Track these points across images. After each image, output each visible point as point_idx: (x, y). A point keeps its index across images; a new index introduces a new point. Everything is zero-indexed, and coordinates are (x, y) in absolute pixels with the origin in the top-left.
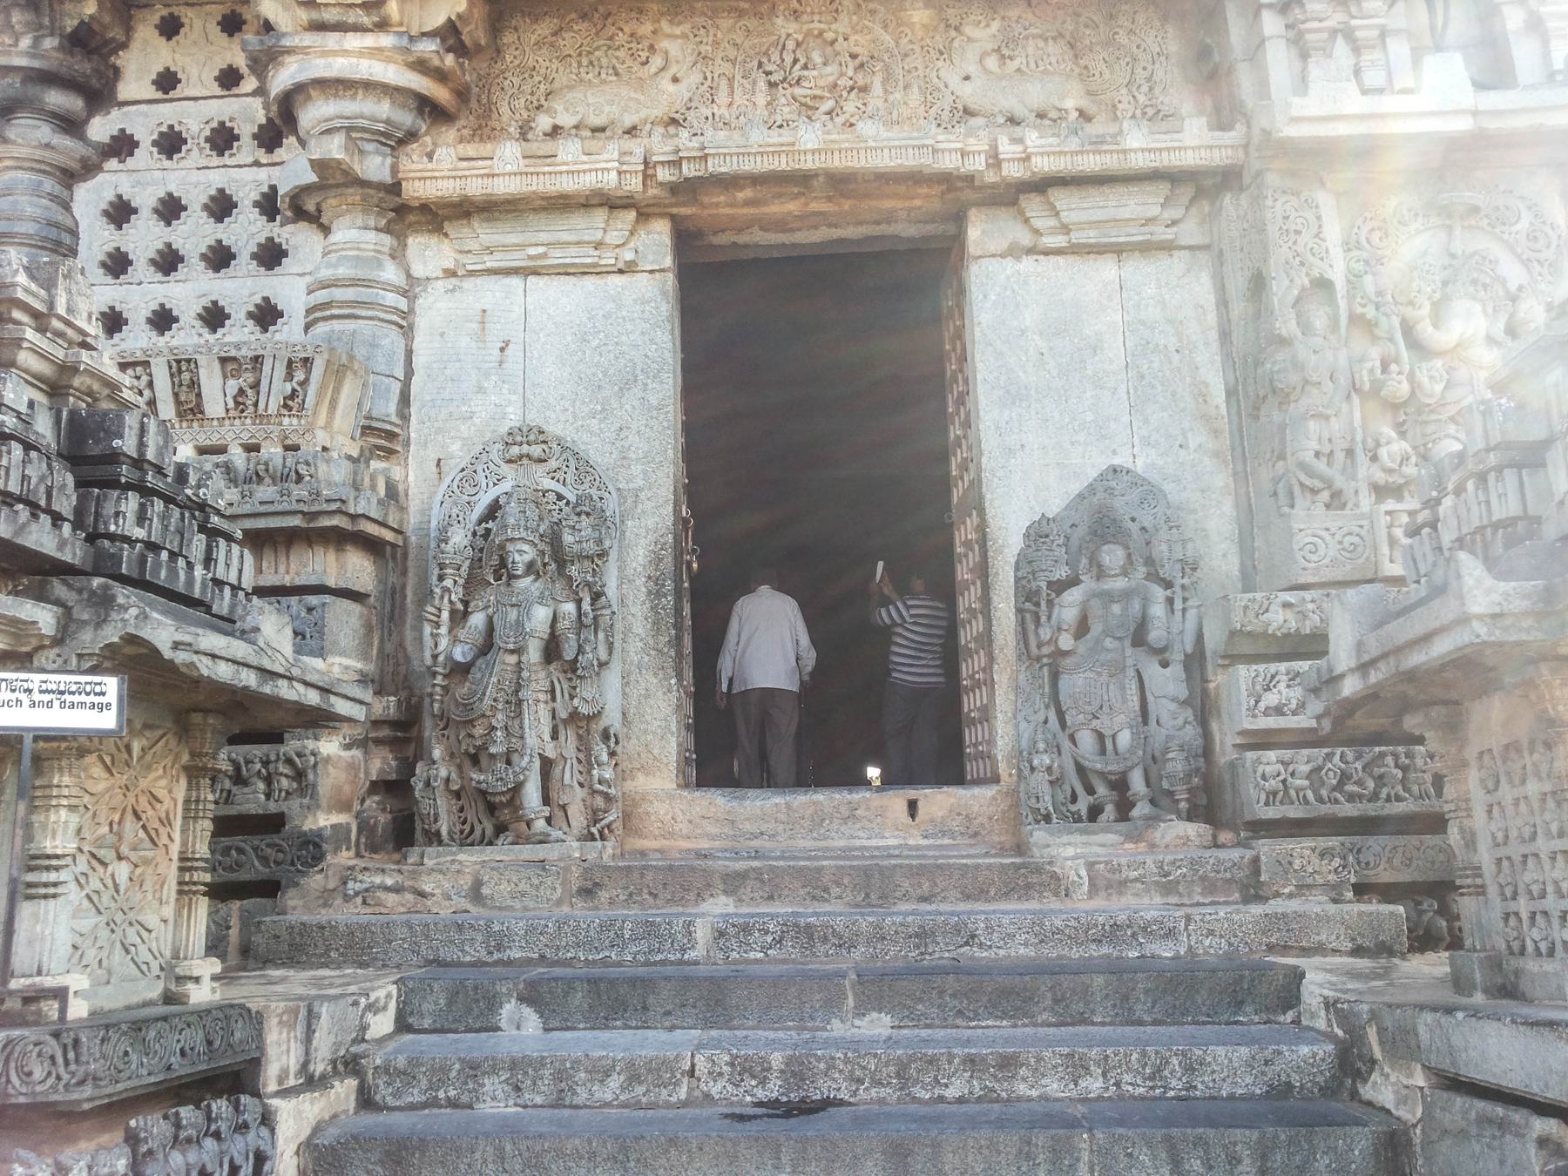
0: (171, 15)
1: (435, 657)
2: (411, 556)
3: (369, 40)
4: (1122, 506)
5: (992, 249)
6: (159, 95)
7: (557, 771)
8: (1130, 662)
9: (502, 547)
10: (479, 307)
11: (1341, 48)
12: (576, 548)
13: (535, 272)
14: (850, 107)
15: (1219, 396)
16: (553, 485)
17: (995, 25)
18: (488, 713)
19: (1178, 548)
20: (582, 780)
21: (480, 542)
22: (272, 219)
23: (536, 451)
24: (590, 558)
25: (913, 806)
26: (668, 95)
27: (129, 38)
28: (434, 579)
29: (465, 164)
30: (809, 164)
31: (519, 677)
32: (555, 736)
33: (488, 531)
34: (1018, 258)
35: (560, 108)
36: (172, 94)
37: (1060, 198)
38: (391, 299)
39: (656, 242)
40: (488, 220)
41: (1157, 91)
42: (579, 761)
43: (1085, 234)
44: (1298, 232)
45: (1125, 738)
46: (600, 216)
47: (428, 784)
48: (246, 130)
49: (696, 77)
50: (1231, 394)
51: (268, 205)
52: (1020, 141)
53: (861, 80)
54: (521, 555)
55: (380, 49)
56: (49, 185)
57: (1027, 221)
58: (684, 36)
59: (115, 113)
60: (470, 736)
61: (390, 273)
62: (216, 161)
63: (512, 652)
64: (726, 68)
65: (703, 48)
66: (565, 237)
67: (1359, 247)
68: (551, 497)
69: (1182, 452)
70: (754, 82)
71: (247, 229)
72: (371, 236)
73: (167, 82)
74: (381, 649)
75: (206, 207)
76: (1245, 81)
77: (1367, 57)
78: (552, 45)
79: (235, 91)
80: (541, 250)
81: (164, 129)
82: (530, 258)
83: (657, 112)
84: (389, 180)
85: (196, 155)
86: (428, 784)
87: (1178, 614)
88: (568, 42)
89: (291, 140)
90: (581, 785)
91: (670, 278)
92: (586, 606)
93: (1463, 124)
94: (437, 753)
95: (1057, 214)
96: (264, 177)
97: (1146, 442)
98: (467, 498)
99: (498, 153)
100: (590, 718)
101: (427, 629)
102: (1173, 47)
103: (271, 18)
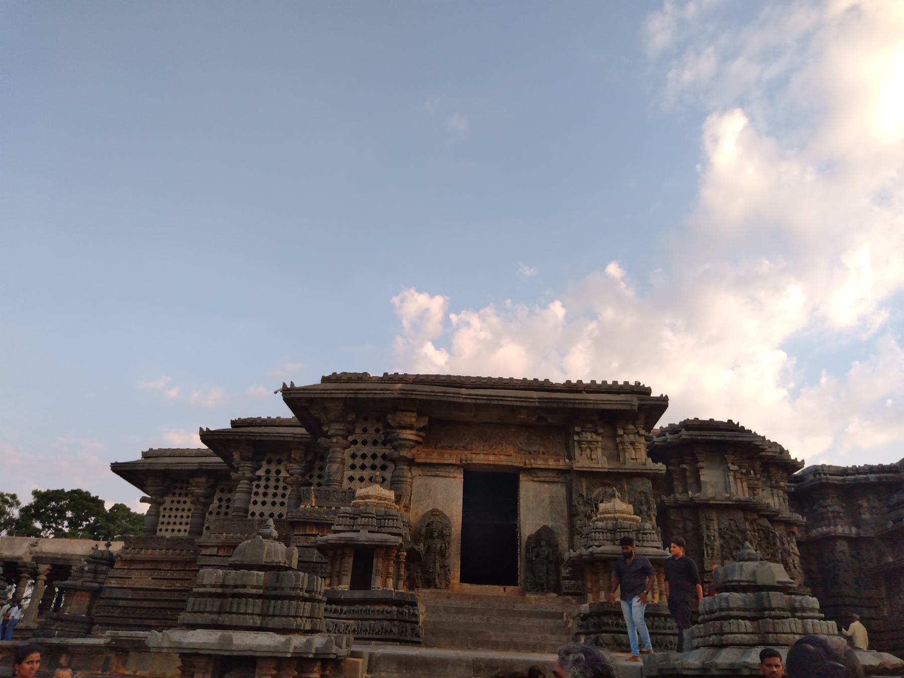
13: (437, 476)
16: (440, 520)
23: (438, 513)
30: (491, 463)
34: (529, 482)
48: (380, 441)
59: (354, 435)
62: (374, 447)
71: (379, 462)
77: (593, 452)
93: (606, 470)
94: (419, 571)
100: (447, 566)
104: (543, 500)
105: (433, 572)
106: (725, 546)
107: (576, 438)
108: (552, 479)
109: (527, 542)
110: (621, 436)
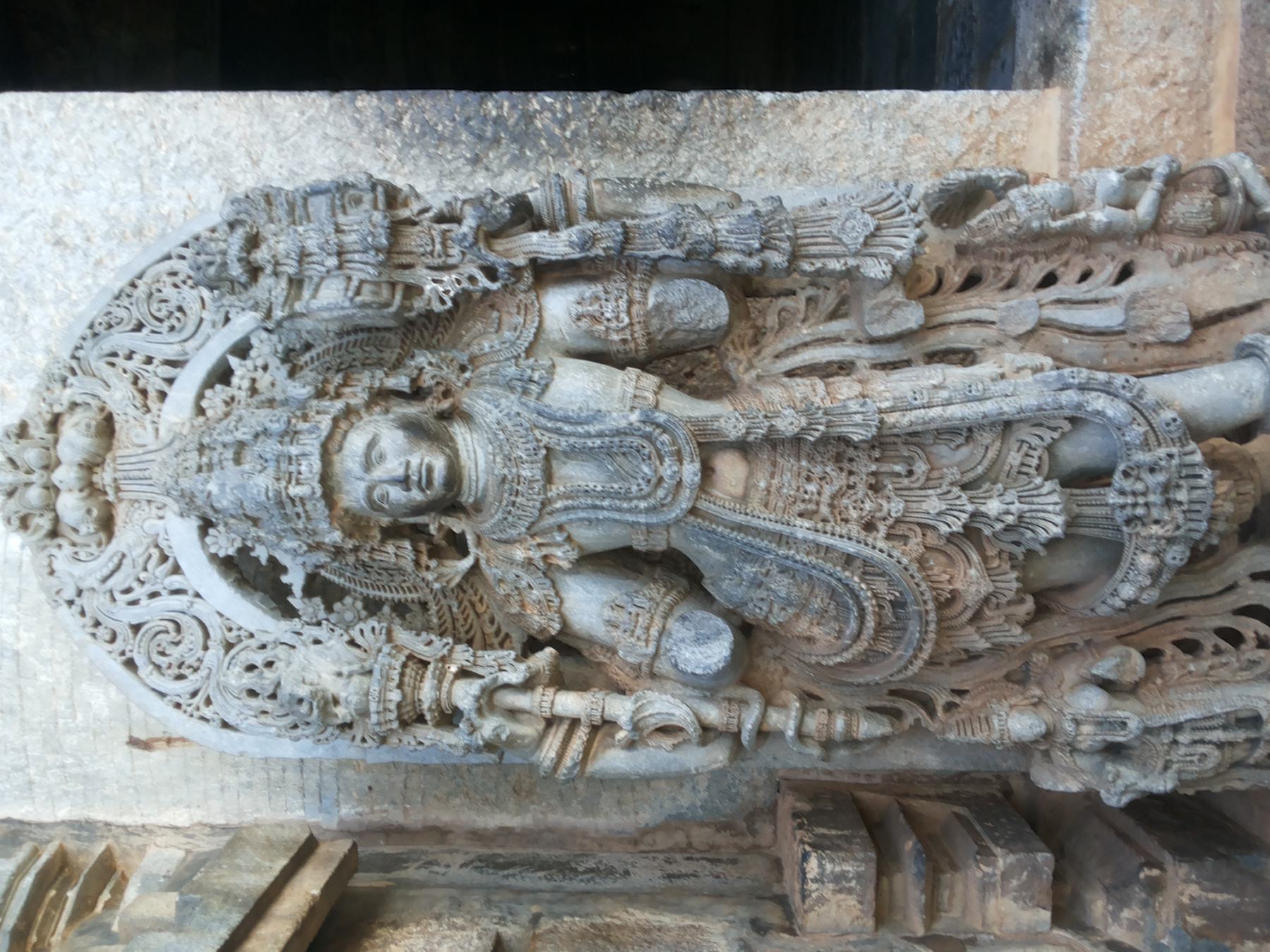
1: (707, 732)
2: (396, 816)
9: (355, 524)
12: (364, 268)
18: (915, 544)
20: (1112, 269)
21: (349, 607)
24: (396, 228)
28: (453, 739)
31: (797, 441)
32: (966, 357)
42: (1049, 280)
63: (707, 471)
74: (654, 899)
86: (1114, 751)
90: (1125, 273)
98: (215, 650)
101: (614, 759)
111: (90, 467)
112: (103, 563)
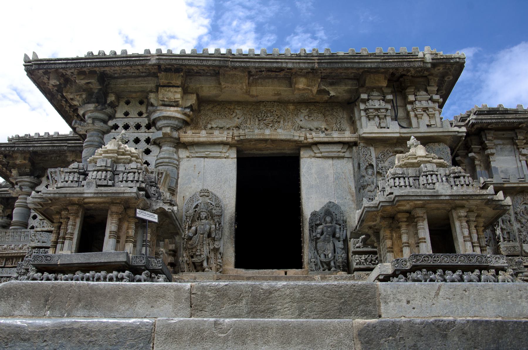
0: (128, 100)
3: (176, 109)
4: (332, 210)
5: (306, 156)
6: (125, 117)
7: (210, 260)
8: (331, 240)
9: (200, 213)
10: (194, 164)
11: (377, 119)
13: (207, 157)
14: (276, 126)
15: (353, 189)
16: (210, 201)
17: (308, 110)
19: (342, 217)
22: (148, 144)
23: (206, 194)
24: (219, 216)
25: (286, 273)
26: (237, 121)
27: (119, 104)
29: (194, 134)
30: (267, 137)
33: (196, 211)
34: (311, 158)
35: (213, 123)
36: (127, 117)
37: (320, 147)
38: (176, 162)
39: (233, 154)
40: (197, 146)
41: (342, 125)
43: (325, 154)
44: (366, 155)
45: (330, 255)
46: (221, 147)
47: (183, 261)
49: (243, 118)
50: (355, 188)
51: (148, 141)
52: (311, 134)
53: (278, 120)
54: (203, 215)
55: (178, 111)
56: (100, 135)
57: (313, 151)
58: (240, 109)
59: (114, 120)
60: (192, 251)
61: (175, 156)
62: (136, 131)
63: (202, 234)
64: (249, 116)
65: (244, 112)
66: (214, 150)
67: (379, 158)
68: (210, 204)
69: (345, 200)
70: (255, 120)
71: (143, 145)
72: (172, 149)
73: (126, 114)
75: (133, 141)
76: (358, 123)
78: (212, 110)
79: (142, 116)
80: (209, 153)
81: (125, 124)
82: (206, 154)
83: (234, 125)
84: (177, 137)
85: (132, 129)
87: (342, 231)
88: (215, 110)
89: (153, 128)
91: (236, 160)
92: (217, 226)
93: (398, 135)
94: (184, 255)
95: (319, 150)
96: (146, 135)
97: (338, 198)
99: (201, 133)
102: (345, 116)
103: (153, 102)
104: (327, 177)
105: (200, 255)
106: (522, 229)
107: (362, 106)
108: (336, 154)
109: (311, 219)
110: (412, 103)
111: (205, 195)
112: (198, 196)
